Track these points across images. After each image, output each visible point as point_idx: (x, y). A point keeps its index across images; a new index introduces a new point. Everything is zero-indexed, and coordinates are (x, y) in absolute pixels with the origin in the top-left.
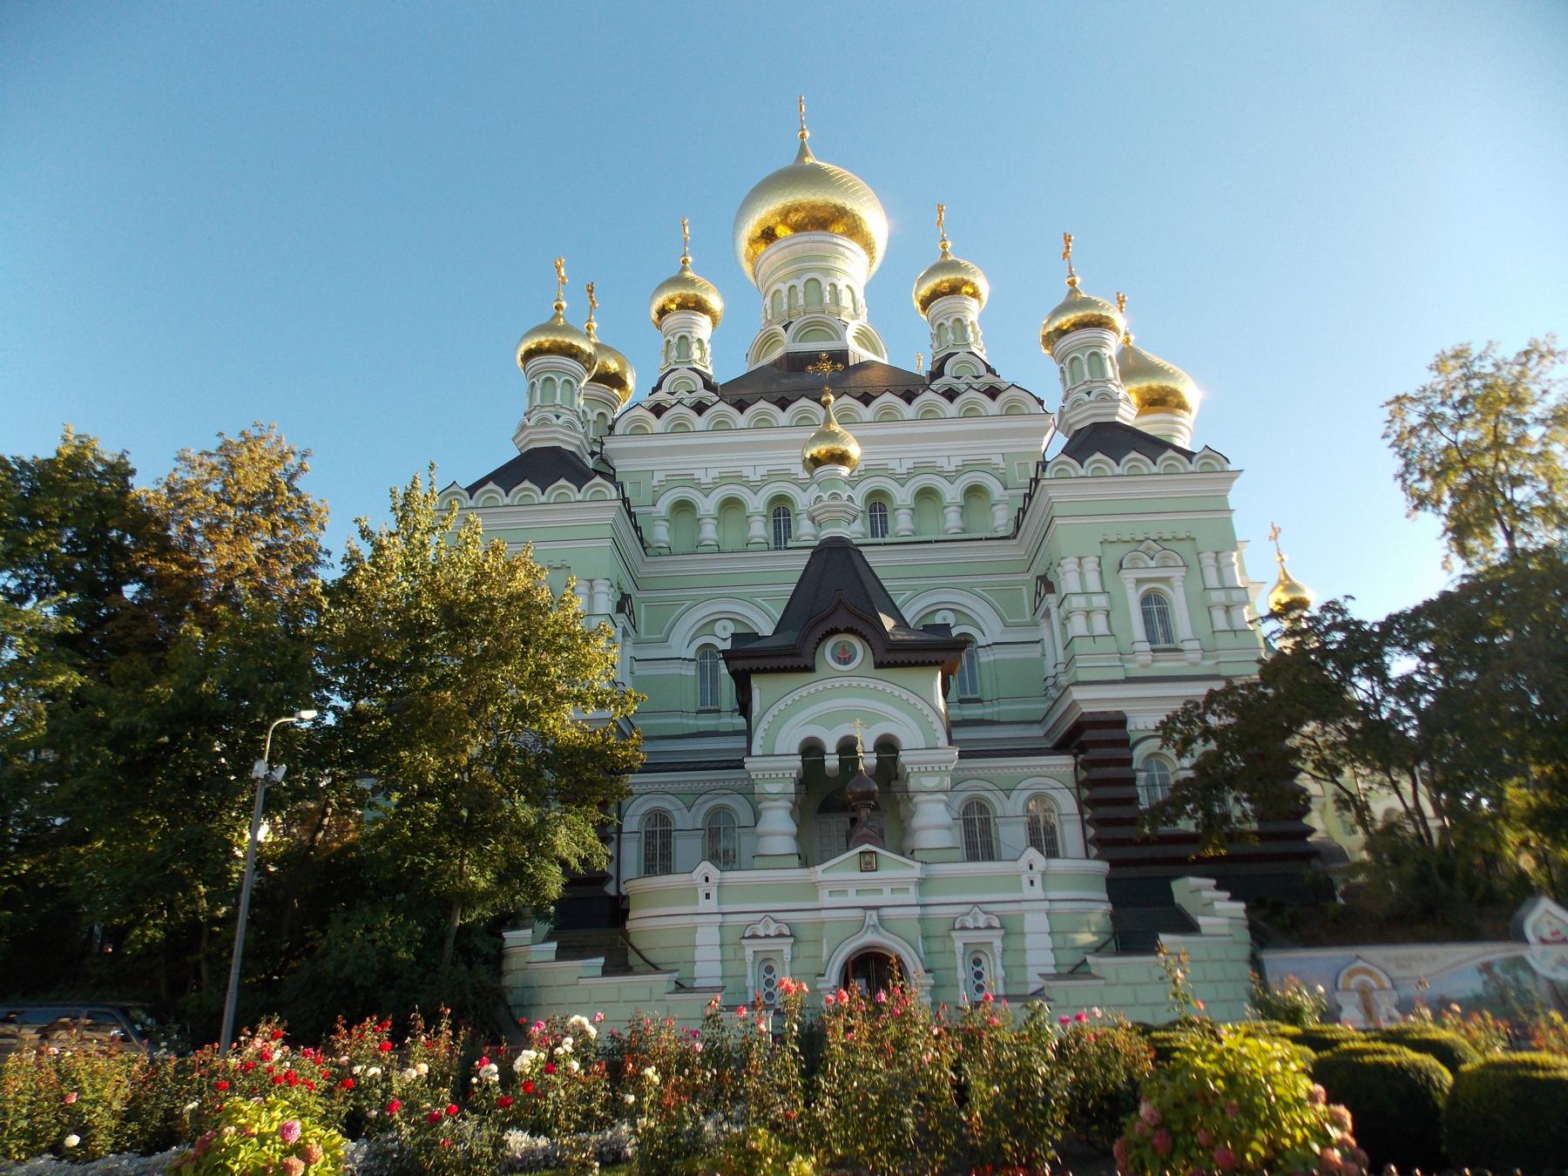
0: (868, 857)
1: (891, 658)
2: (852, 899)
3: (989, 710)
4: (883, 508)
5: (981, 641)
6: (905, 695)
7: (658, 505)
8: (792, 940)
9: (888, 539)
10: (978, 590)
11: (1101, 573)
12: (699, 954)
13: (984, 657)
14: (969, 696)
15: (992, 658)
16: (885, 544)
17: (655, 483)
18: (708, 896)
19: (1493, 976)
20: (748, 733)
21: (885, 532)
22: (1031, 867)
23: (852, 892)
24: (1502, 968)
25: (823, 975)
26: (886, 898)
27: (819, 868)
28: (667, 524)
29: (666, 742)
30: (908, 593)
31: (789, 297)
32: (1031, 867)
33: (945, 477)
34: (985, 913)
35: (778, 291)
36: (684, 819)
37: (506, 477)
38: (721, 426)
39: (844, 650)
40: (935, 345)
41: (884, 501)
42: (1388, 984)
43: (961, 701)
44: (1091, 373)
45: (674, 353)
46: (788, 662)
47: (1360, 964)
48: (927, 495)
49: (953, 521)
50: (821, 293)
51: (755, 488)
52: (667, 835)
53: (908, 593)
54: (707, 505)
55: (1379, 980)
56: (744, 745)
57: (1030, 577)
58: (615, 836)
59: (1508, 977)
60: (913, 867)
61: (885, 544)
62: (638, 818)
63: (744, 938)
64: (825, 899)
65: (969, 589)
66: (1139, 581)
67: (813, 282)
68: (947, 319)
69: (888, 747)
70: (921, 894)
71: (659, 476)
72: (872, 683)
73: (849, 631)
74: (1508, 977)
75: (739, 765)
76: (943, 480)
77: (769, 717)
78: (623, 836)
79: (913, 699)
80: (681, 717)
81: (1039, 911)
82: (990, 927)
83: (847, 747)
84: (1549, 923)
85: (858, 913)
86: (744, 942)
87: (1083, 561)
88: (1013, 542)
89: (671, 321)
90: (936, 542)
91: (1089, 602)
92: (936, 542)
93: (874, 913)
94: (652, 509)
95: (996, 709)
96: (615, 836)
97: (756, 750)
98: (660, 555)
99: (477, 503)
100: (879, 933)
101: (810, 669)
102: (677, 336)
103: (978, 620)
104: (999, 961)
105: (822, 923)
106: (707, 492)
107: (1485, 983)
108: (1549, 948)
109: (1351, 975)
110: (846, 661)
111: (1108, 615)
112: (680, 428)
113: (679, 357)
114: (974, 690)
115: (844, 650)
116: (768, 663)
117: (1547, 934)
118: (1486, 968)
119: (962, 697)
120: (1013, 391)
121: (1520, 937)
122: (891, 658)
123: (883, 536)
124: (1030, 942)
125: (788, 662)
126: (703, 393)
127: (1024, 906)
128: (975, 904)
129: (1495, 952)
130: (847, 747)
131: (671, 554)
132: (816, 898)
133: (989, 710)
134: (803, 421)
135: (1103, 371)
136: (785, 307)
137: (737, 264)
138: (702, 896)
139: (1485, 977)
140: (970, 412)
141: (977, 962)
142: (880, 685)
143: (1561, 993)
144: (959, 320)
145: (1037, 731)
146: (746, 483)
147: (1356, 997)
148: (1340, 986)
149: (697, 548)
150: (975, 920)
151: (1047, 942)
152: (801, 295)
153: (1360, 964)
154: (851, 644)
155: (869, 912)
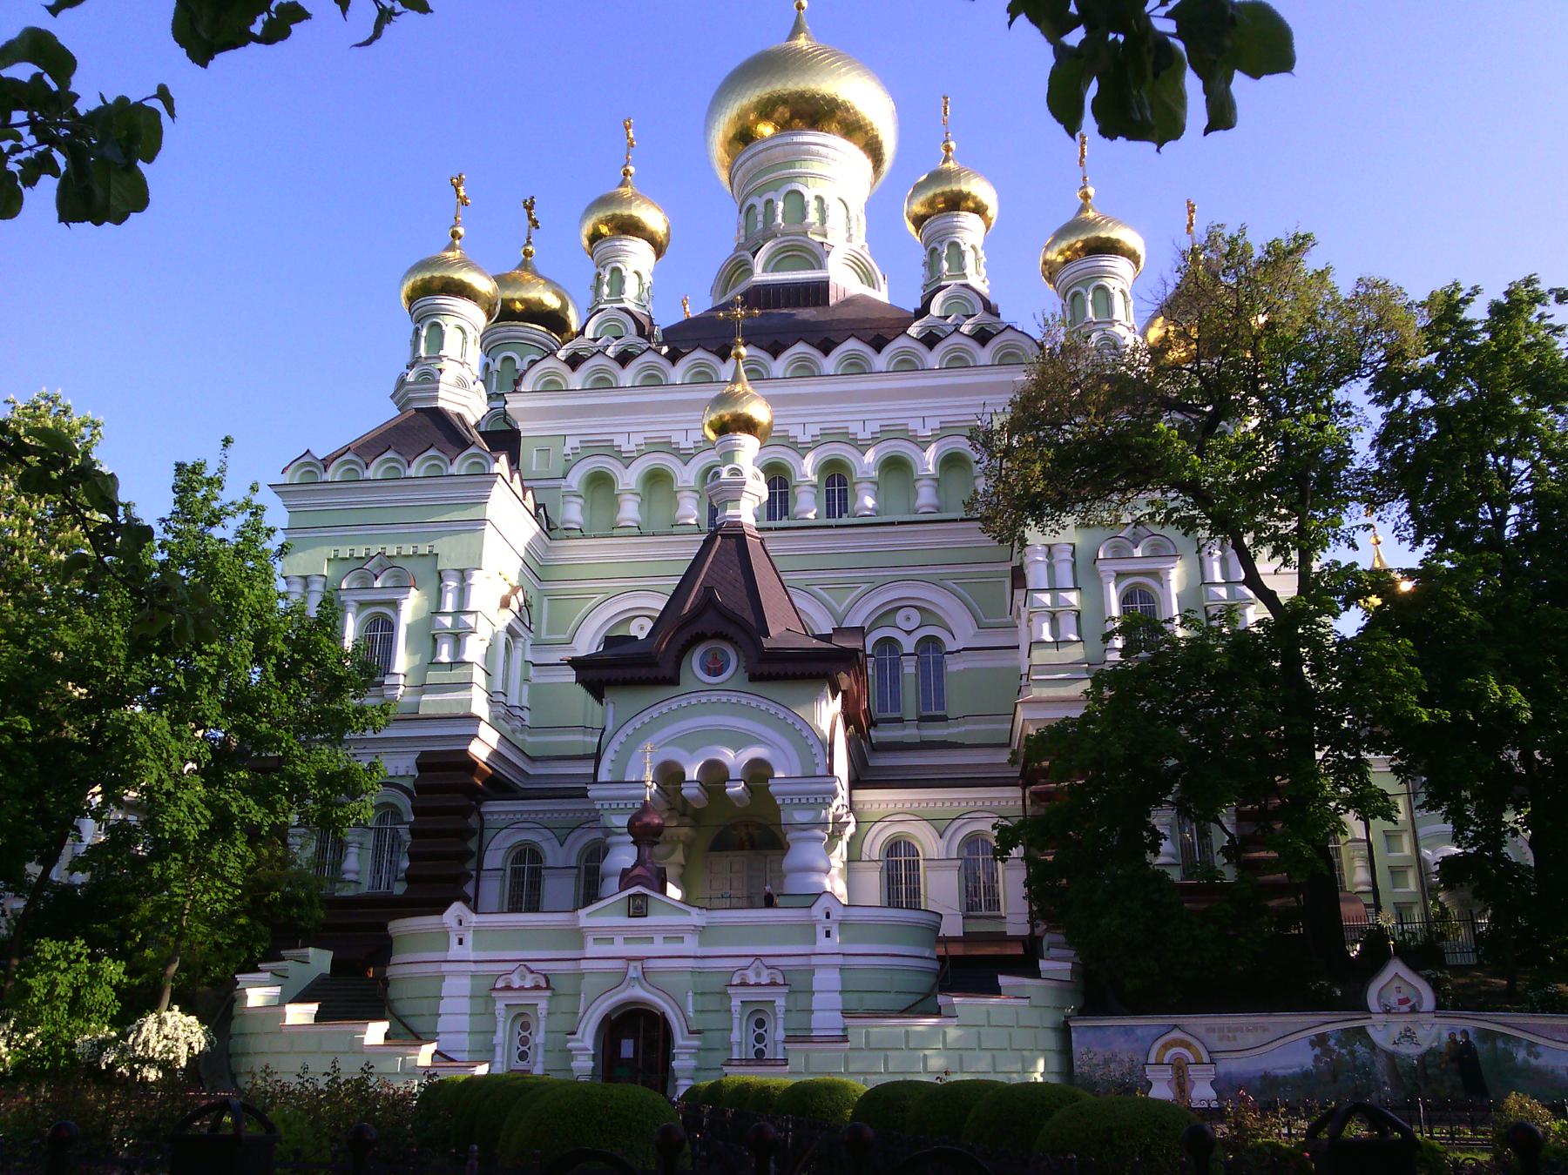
0: (639, 901)
1: (765, 668)
2: (620, 948)
4: (843, 482)
5: (951, 645)
8: (548, 993)
9: (845, 520)
11: (1074, 564)
12: (445, 1006)
13: (953, 666)
14: (934, 712)
15: (961, 666)
16: (837, 526)
17: (567, 450)
18: (461, 941)
19: (1327, 1051)
20: (597, 757)
21: (844, 509)
22: (828, 916)
23: (619, 940)
24: (1338, 1041)
25: (575, 1033)
26: (659, 947)
27: (582, 913)
28: (580, 501)
29: (563, 763)
30: (864, 586)
31: (765, 216)
32: (828, 916)
34: (768, 968)
35: (752, 207)
36: (553, 854)
37: (370, 447)
38: (653, 380)
39: (715, 659)
40: (928, 274)
42: (1206, 1059)
43: (922, 719)
44: (1096, 313)
46: (643, 673)
47: (1176, 1034)
48: (895, 466)
49: (926, 496)
51: (686, 457)
52: (536, 875)
54: (629, 479)
55: (1196, 1053)
56: (592, 771)
57: (1007, 567)
58: (474, 873)
59: (1344, 1051)
60: (689, 913)
61: (837, 526)
62: (503, 852)
63: (494, 989)
64: (592, 949)
65: (938, 583)
66: (1120, 576)
67: (791, 196)
68: (941, 243)
69: (758, 772)
70: (701, 944)
71: (573, 442)
73: (719, 636)
74: (1344, 1051)
75: (582, 794)
76: (911, 445)
77: (621, 737)
78: (483, 873)
80: (585, 734)
81: (834, 965)
82: (773, 984)
83: (715, 772)
84: (1399, 990)
85: (620, 964)
86: (494, 994)
89: (602, 247)
91: (1055, 600)
93: (638, 964)
94: (563, 482)
95: (963, 729)
96: (474, 873)
97: (604, 775)
98: (568, 538)
99: (334, 475)
100: (642, 986)
101: (674, 681)
103: (948, 620)
104: (780, 1023)
105: (581, 975)
106: (628, 461)
107: (1317, 1058)
108: (1391, 1018)
109: (1166, 1047)
110: (716, 672)
111: (1078, 618)
112: (602, 383)
113: (610, 295)
114: (941, 705)
115: (715, 659)
116: (628, 673)
117: (1393, 1000)
118: (1320, 1040)
119: (925, 713)
120: (1008, 335)
121: (1361, 1007)
122: (765, 668)
123: (840, 516)
124: (818, 1001)
125: (643, 673)
126: (631, 337)
127: (815, 960)
128: (758, 957)
129: (1332, 1024)
130: (715, 772)
131: (584, 537)
132: (582, 946)
134: (703, 377)
135: (1110, 310)
136: (760, 226)
137: (712, 170)
138: (454, 941)
139: (1317, 1050)
140: (958, 362)
141: (760, 1023)
143: (1400, 1070)
145: (1003, 757)
146: (676, 452)
147: (1169, 1073)
148: (1152, 1059)
149: (613, 529)
150: (758, 974)
151: (836, 1000)
153: (1176, 1034)
155: (633, 964)
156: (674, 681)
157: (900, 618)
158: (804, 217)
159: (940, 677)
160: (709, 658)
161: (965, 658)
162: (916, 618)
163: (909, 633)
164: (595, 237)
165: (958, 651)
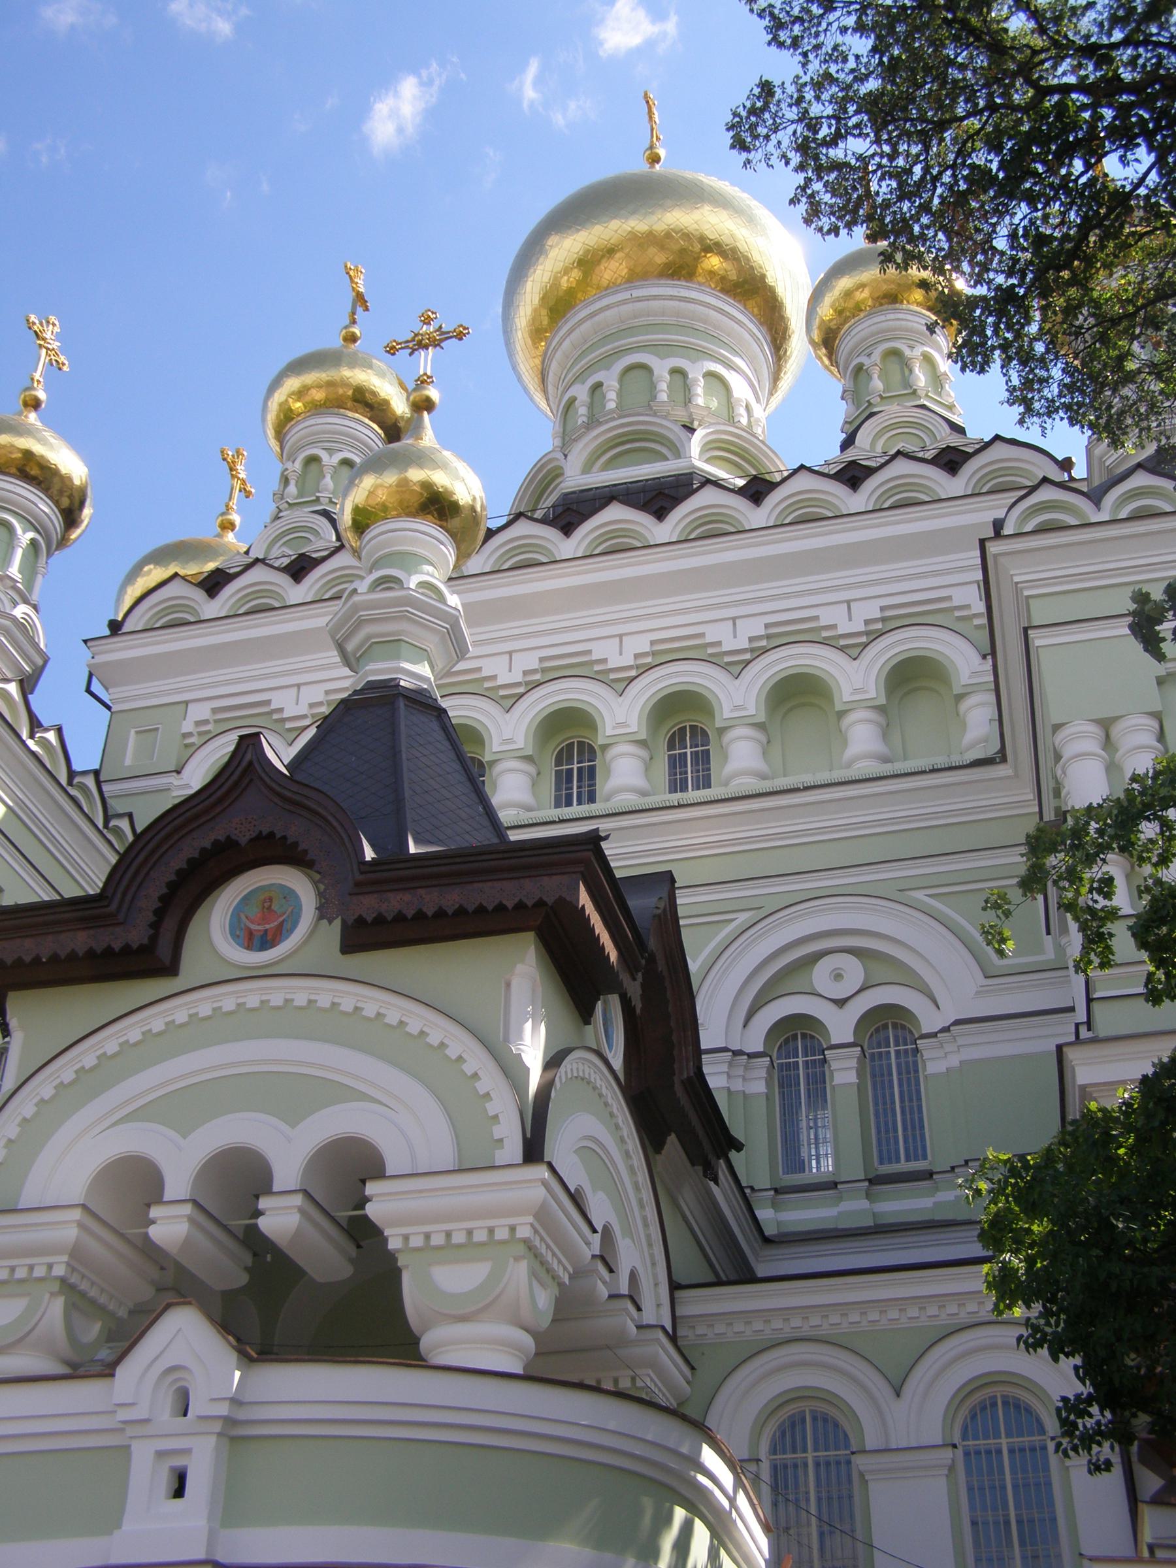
1: (369, 906)
3: (947, 1196)
4: (700, 735)
5: (929, 1020)
6: (417, 1019)
7: (186, 772)
10: (920, 895)
14: (904, 1166)
15: (954, 1061)
17: (188, 726)
33: (842, 649)
35: (572, 401)
39: (267, 910)
41: (700, 721)
45: (292, 489)
50: (652, 387)
53: (743, 918)
65: (898, 896)
71: (199, 712)
72: (348, 996)
79: (439, 1030)
87: (1116, 731)
88: (1001, 771)
90: (807, 788)
92: (807, 788)
94: (173, 780)
102: (301, 457)
110: (266, 941)
114: (917, 1150)
115: (267, 910)
133: (947, 1196)
142: (372, 1002)
144: (895, 353)
152: (612, 395)
154: (289, 895)
156: (171, 969)
157: (821, 974)
158: (654, 397)
159: (912, 1095)
160: (254, 911)
161: (960, 1041)
162: (854, 972)
163: (841, 1003)
164: (287, 418)
165: (946, 1030)
